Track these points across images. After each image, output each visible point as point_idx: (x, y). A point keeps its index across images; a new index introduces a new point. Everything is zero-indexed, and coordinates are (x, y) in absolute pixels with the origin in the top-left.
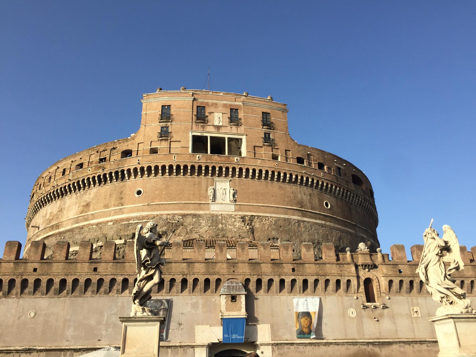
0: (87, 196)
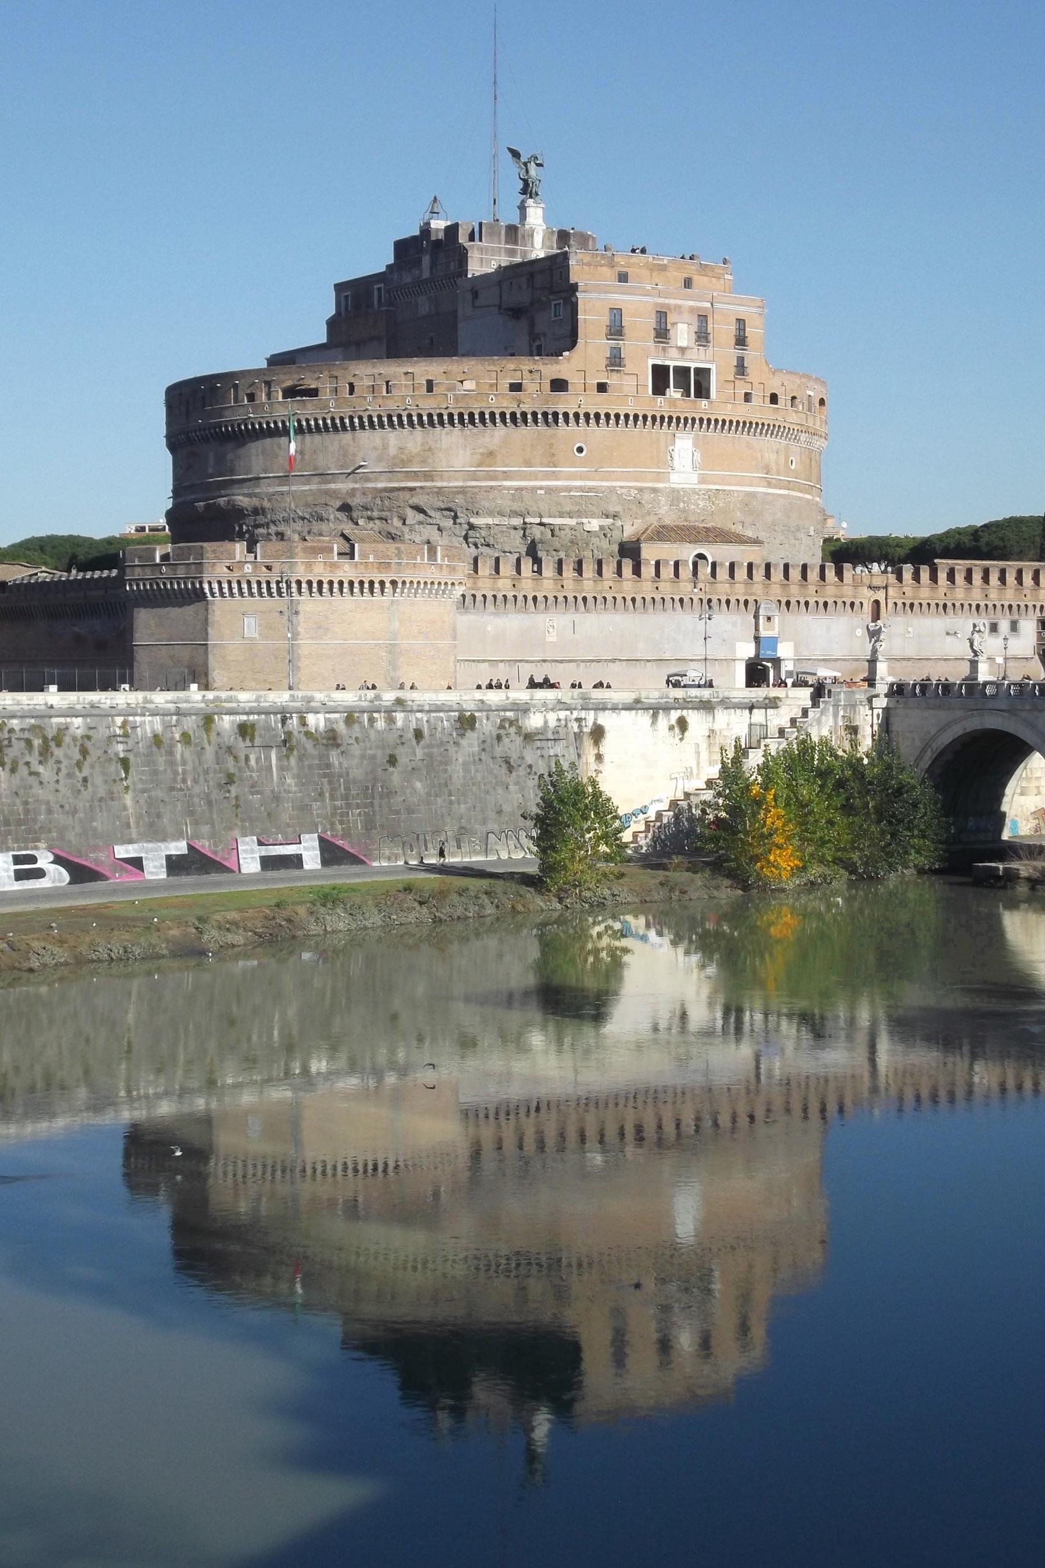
0: (487, 439)
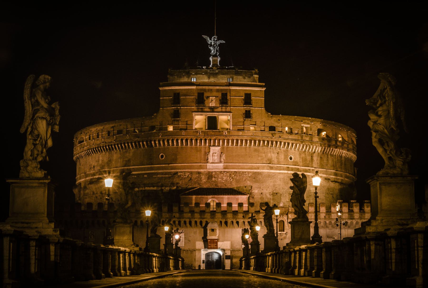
0: (128, 154)
